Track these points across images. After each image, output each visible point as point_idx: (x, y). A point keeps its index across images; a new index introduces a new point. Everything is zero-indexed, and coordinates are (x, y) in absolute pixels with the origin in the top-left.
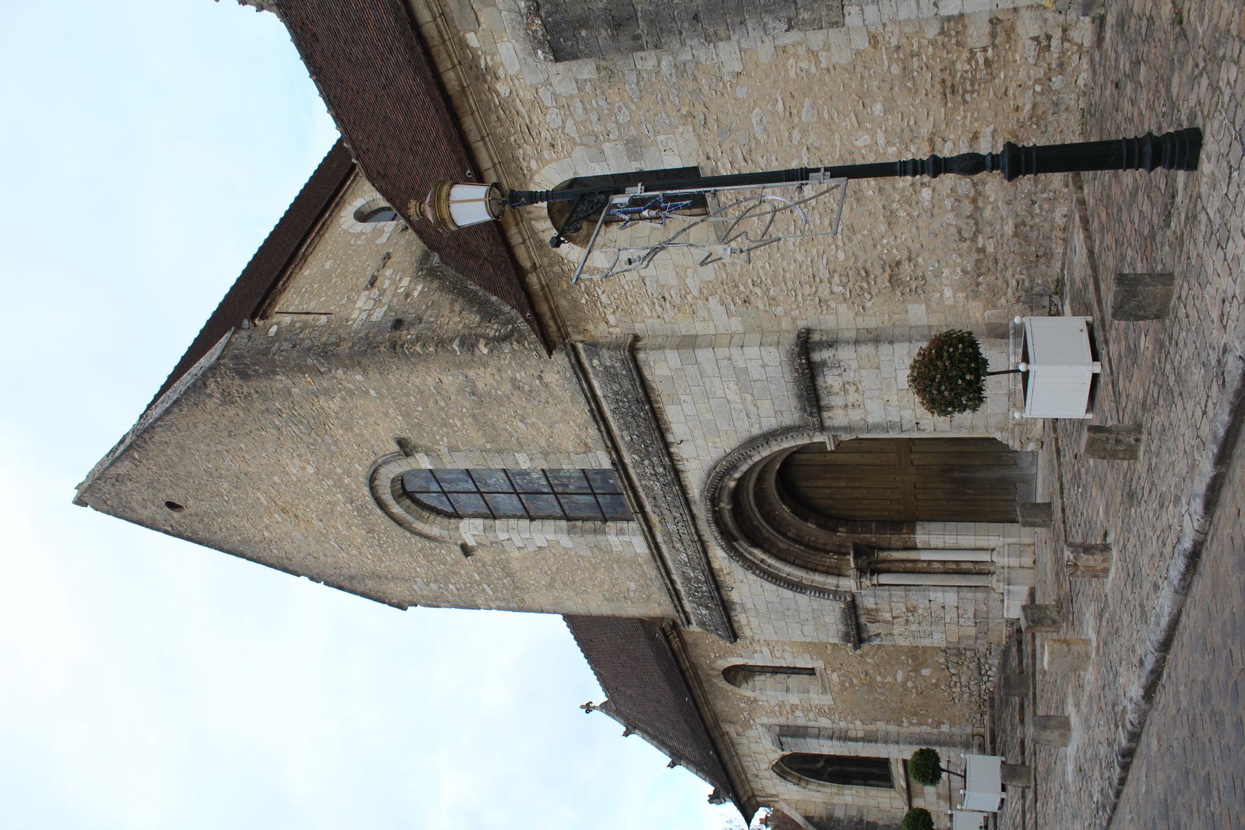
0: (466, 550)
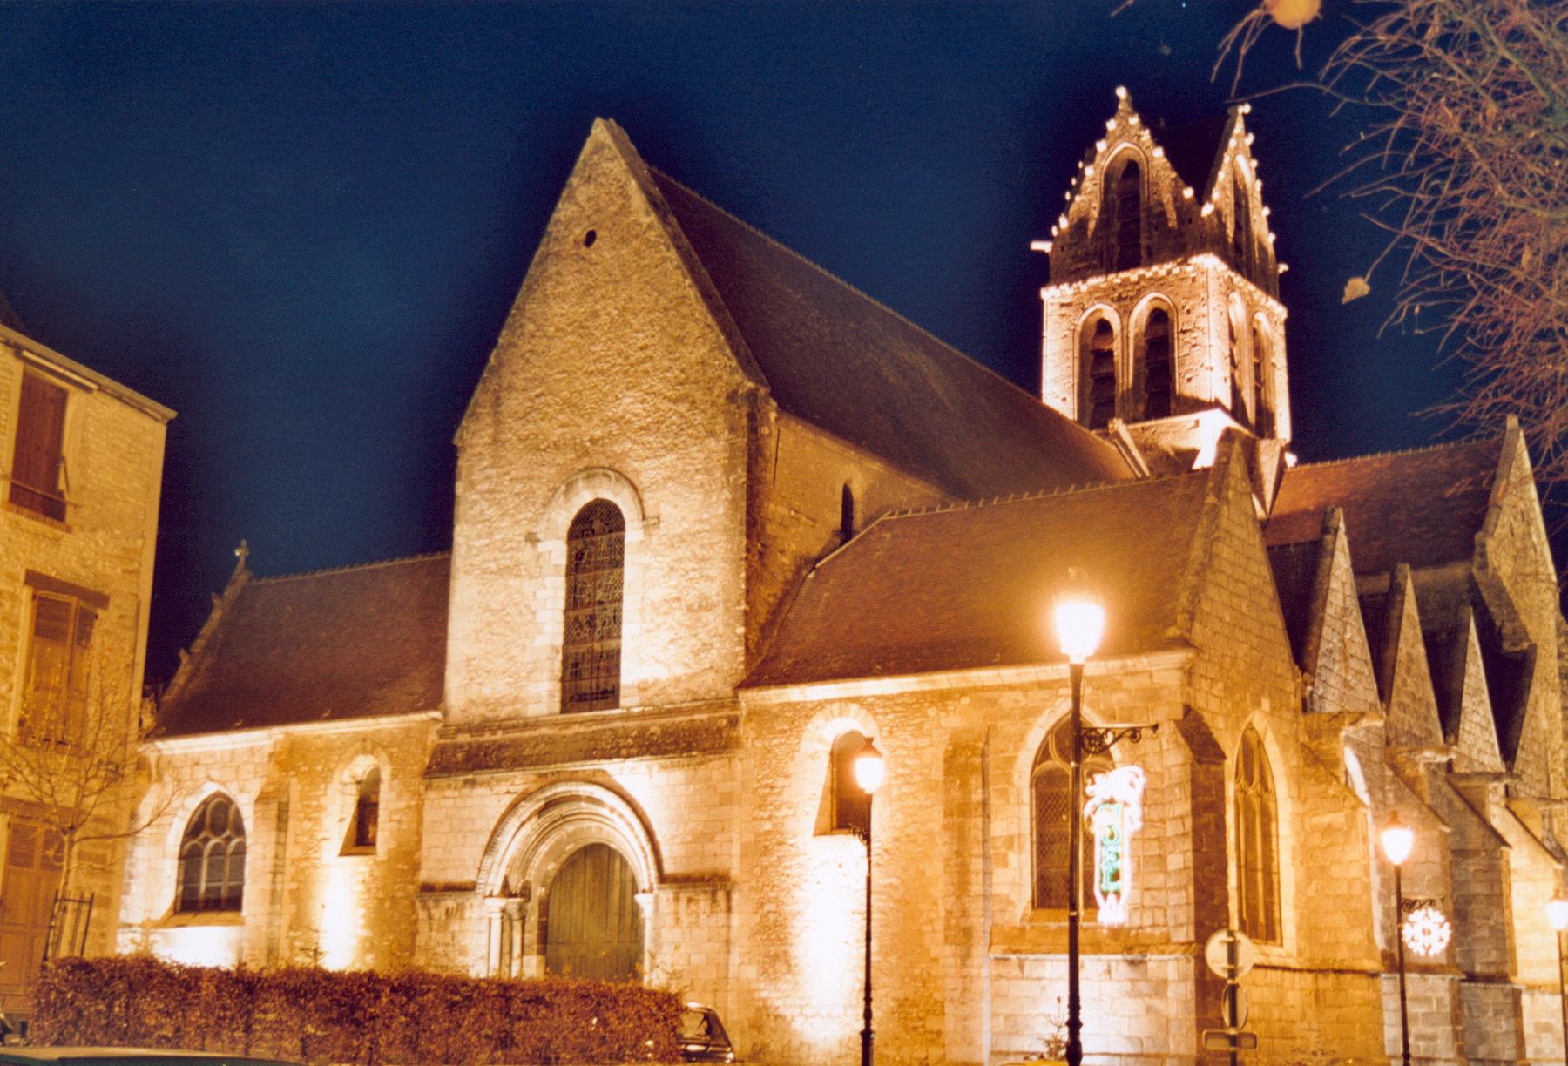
0: (532, 539)
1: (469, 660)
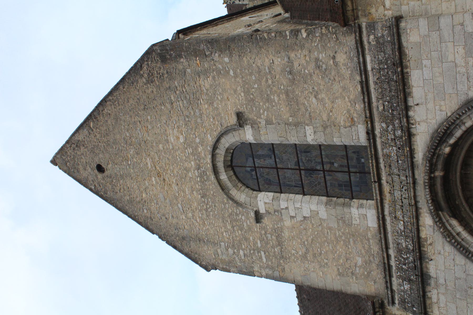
0: (258, 217)
1: (340, 274)
